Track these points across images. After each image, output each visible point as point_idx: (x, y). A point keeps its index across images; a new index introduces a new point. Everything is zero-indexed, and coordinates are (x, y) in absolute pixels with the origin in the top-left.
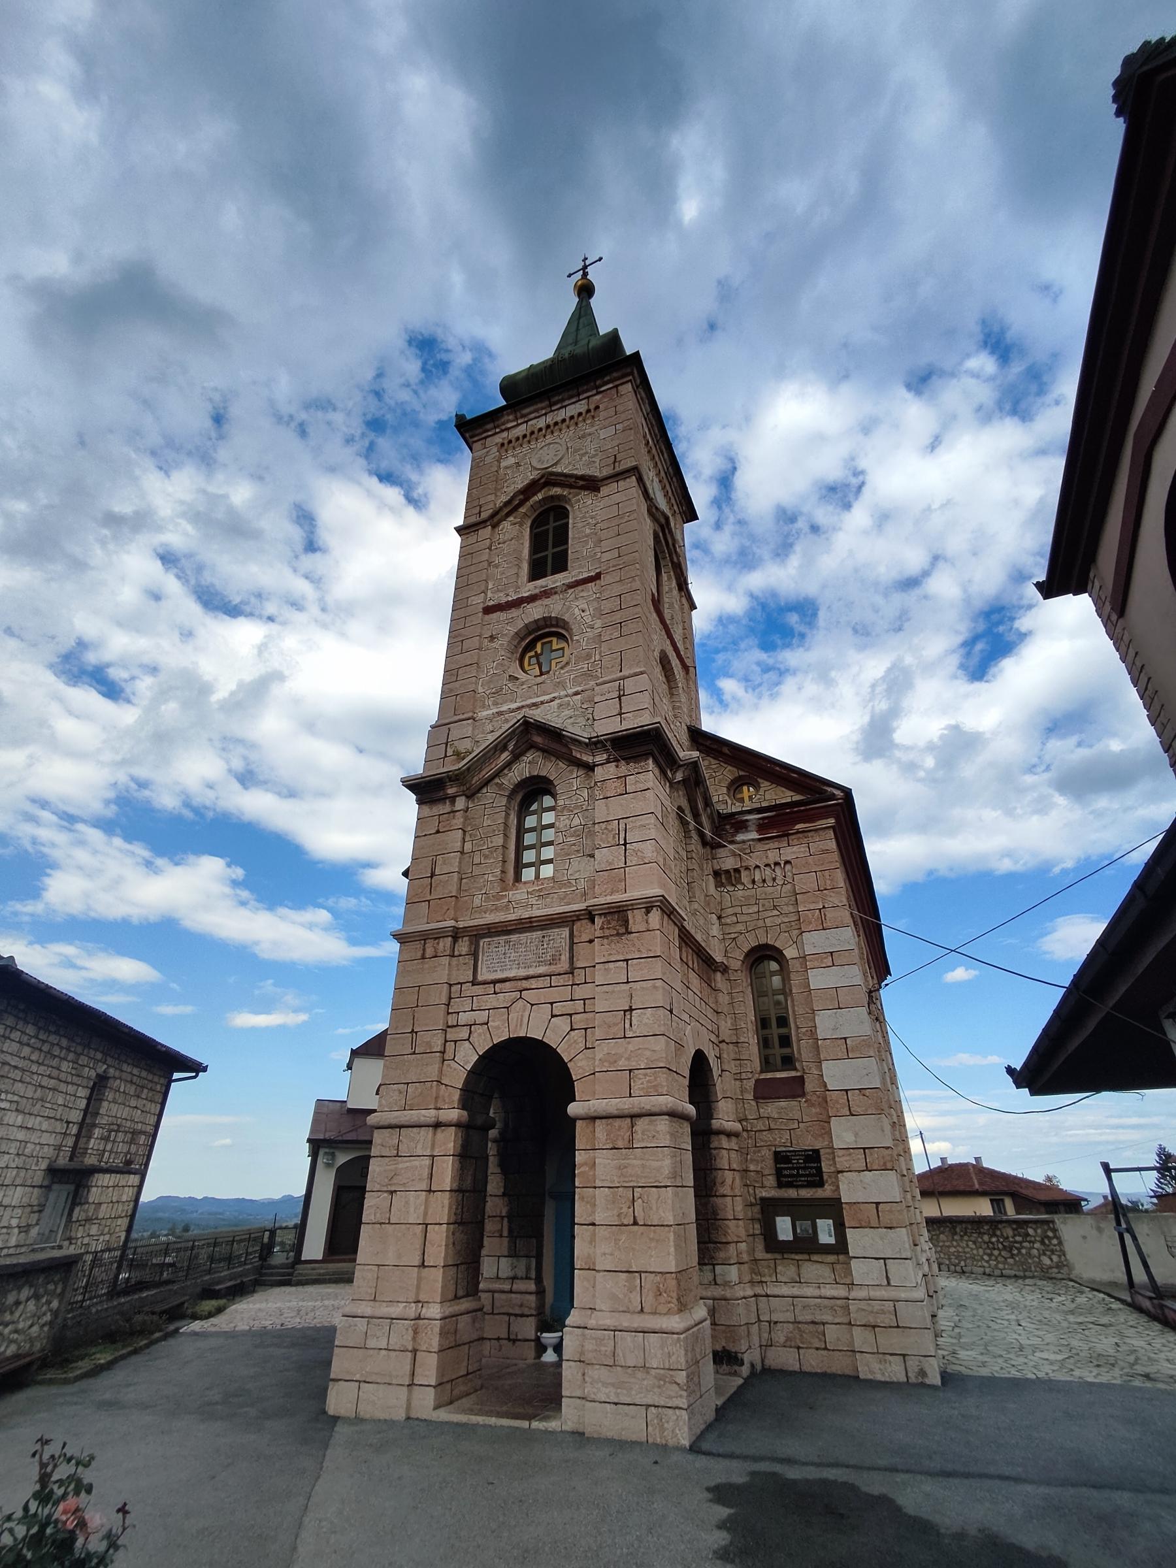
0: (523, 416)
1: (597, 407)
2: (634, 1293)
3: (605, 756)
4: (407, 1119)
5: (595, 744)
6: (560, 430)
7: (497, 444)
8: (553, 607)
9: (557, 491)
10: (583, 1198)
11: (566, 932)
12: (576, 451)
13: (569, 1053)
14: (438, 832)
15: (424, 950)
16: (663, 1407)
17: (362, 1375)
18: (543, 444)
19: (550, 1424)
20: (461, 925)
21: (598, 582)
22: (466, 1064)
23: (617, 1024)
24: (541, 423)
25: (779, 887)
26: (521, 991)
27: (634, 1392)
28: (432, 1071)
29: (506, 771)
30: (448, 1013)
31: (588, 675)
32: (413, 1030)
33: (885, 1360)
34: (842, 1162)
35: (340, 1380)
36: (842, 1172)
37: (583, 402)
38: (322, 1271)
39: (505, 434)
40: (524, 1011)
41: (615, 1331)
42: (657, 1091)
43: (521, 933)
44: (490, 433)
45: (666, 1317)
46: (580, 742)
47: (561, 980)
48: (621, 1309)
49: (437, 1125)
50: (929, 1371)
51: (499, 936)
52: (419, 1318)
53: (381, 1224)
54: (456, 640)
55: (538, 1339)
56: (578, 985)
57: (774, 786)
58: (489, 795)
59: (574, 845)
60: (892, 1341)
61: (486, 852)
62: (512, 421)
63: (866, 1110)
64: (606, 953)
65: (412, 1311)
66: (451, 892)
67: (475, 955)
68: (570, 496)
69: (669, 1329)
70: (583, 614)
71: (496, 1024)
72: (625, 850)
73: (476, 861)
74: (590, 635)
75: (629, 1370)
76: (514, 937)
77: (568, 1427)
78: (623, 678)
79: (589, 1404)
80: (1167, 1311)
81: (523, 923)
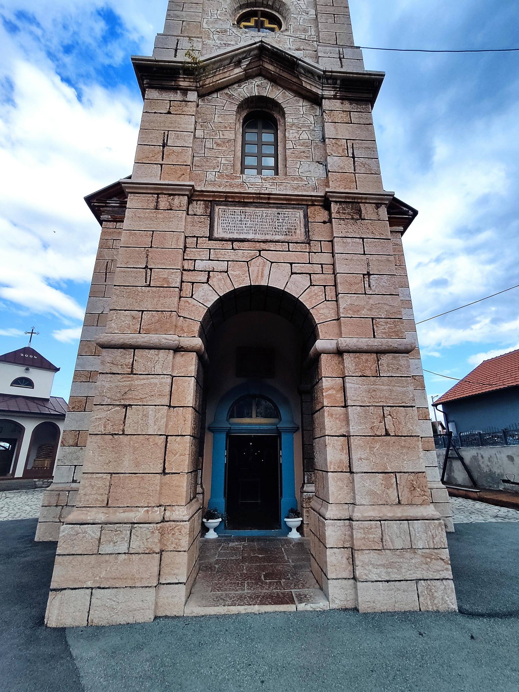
2: (391, 490)
3: (332, 93)
11: (300, 214)
13: (311, 302)
14: (169, 113)
15: (157, 202)
17: (95, 581)
19: (318, 605)
22: (206, 302)
26: (260, 251)
27: (404, 570)
28: (172, 302)
29: (235, 86)
30: (184, 259)
32: (146, 267)
35: (65, 589)
40: (264, 266)
41: (380, 521)
43: (257, 207)
47: (299, 247)
48: (380, 503)
49: (178, 349)
52: (163, 521)
55: (203, 523)
56: (315, 253)
59: (304, 152)
61: (219, 141)
64: (343, 231)
65: (157, 514)
66: (185, 162)
69: (430, 516)
71: (237, 273)
72: (354, 161)
73: (208, 145)
74: (306, 17)
76: (249, 210)
77: (336, 604)
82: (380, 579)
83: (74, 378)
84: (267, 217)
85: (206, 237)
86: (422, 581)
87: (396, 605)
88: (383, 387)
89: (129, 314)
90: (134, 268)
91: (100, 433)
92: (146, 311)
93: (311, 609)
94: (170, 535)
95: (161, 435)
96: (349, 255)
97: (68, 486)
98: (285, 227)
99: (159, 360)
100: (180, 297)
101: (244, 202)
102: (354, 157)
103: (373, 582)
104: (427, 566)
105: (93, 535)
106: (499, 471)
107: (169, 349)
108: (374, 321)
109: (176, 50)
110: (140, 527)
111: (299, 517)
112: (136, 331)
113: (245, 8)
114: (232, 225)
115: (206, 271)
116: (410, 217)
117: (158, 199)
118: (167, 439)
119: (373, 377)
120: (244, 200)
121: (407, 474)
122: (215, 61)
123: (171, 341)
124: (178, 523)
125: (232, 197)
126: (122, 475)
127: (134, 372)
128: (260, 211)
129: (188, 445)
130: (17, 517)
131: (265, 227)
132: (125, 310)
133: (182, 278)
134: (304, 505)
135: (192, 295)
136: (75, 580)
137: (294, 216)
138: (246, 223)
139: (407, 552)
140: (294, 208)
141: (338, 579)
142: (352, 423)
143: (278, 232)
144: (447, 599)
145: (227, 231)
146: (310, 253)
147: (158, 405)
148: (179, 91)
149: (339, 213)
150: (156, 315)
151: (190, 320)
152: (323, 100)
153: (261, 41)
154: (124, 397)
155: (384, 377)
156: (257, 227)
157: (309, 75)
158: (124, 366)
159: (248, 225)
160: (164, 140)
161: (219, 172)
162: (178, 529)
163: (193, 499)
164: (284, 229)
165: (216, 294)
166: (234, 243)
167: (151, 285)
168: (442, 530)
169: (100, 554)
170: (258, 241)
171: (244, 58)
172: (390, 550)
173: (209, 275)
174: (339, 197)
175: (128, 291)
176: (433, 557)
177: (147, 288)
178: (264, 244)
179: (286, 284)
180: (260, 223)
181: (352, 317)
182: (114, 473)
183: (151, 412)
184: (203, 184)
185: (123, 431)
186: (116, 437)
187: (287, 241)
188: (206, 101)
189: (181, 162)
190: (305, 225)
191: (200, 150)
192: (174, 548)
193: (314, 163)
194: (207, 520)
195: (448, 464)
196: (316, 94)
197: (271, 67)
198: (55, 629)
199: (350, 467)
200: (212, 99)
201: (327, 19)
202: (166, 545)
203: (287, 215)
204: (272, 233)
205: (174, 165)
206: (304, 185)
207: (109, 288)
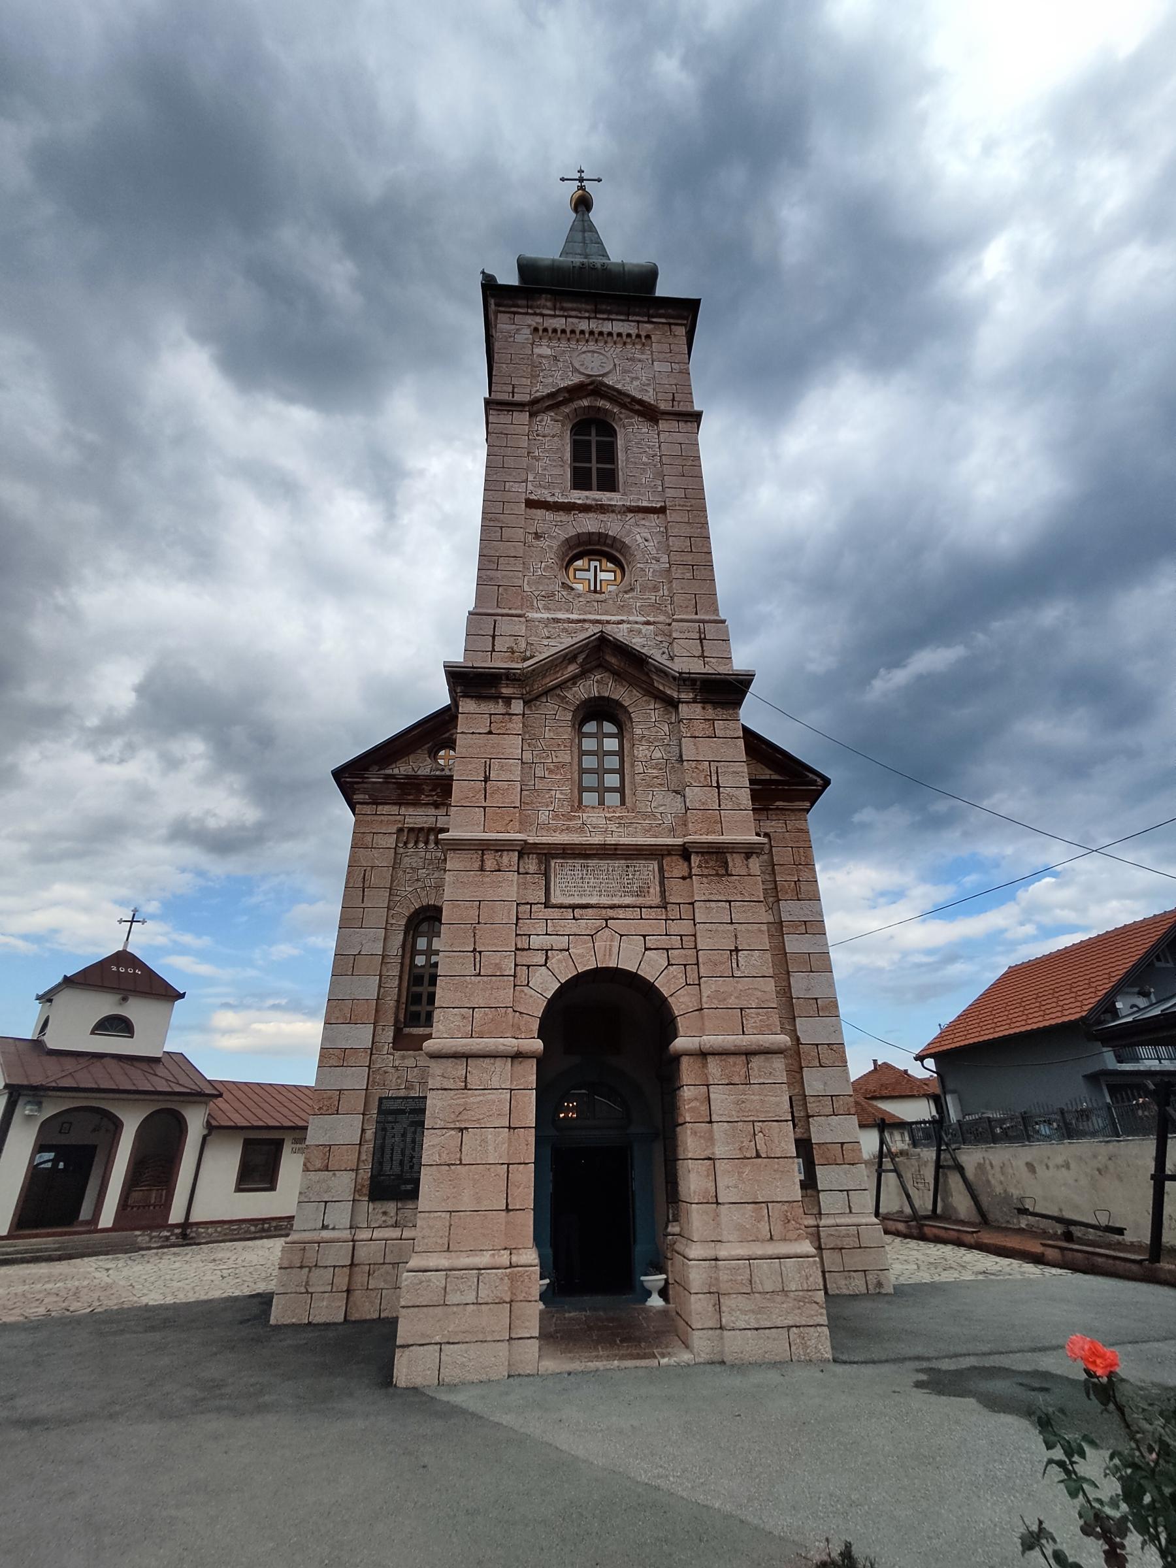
0: (562, 309)
1: (648, 337)
3: (691, 695)
5: (686, 680)
6: (606, 342)
7: (529, 326)
8: (612, 526)
9: (601, 403)
10: (696, 1133)
11: (654, 865)
12: (625, 371)
14: (490, 733)
15: (482, 861)
16: (804, 1326)
18: (585, 349)
20: (531, 840)
21: (660, 515)
22: (545, 992)
24: (584, 325)
26: (606, 920)
28: (505, 995)
29: (569, 684)
31: (657, 607)
32: (475, 950)
33: (850, 1277)
34: (812, 1107)
35: (412, 1345)
36: (813, 1116)
37: (633, 324)
39: (539, 319)
40: (612, 940)
42: (771, 1030)
44: (520, 310)
46: (666, 674)
47: (653, 913)
48: (751, 1239)
49: (518, 1056)
50: (884, 1282)
51: (575, 858)
53: (448, 1165)
54: (492, 524)
56: (673, 920)
57: (754, 762)
58: (549, 707)
59: (656, 777)
60: (856, 1260)
62: (548, 309)
63: (834, 1062)
64: (706, 892)
65: (504, 1258)
66: (513, 802)
67: (546, 875)
68: (622, 416)
70: (646, 544)
73: (539, 773)
75: (768, 1296)
76: (592, 863)
78: (704, 622)
79: (725, 1332)
80: (926, 1230)
81: (607, 849)
82: (748, 1327)
83: (320, 1060)
86: (794, 1328)
87: (766, 1356)
88: (752, 1096)
91: (435, 1163)
93: (675, 1364)
94: (519, 1283)
95: (502, 1164)
97: (315, 1236)
100: (515, 986)
102: (718, 787)
103: (740, 1330)
104: (800, 1311)
105: (438, 1283)
106: (1018, 1192)
107: (506, 1057)
109: (494, 637)
110: (488, 1274)
111: (661, 1274)
112: (468, 1034)
113: (575, 549)
115: (543, 950)
116: (819, 788)
117: (482, 857)
122: (545, 663)
124: (527, 1269)
126: (462, 1213)
127: (469, 1087)
128: (604, 864)
130: (182, 1298)
132: (454, 1008)
134: (669, 1254)
135: (528, 982)
136: (423, 1335)
139: (778, 1295)
144: (821, 1347)
148: (500, 701)
149: (702, 867)
152: (680, 705)
153: (602, 631)
154: (459, 1119)
157: (662, 674)
158: (457, 1080)
159: (591, 884)
160: (485, 772)
168: (817, 1270)
171: (581, 652)
172: (760, 1293)
173: (547, 955)
174: (700, 848)
176: (807, 1300)
182: (454, 1212)
183: (490, 1136)
184: (535, 829)
185: (461, 1160)
186: (453, 1167)
188: (533, 708)
189: (508, 803)
190: (660, 883)
191: (529, 781)
193: (668, 792)
195: (941, 1180)
196: (672, 698)
197: (613, 660)
198: (407, 1388)
199: (716, 1196)
200: (540, 705)
201: (682, 573)
202: (515, 1294)
205: (499, 807)
207: (368, 912)
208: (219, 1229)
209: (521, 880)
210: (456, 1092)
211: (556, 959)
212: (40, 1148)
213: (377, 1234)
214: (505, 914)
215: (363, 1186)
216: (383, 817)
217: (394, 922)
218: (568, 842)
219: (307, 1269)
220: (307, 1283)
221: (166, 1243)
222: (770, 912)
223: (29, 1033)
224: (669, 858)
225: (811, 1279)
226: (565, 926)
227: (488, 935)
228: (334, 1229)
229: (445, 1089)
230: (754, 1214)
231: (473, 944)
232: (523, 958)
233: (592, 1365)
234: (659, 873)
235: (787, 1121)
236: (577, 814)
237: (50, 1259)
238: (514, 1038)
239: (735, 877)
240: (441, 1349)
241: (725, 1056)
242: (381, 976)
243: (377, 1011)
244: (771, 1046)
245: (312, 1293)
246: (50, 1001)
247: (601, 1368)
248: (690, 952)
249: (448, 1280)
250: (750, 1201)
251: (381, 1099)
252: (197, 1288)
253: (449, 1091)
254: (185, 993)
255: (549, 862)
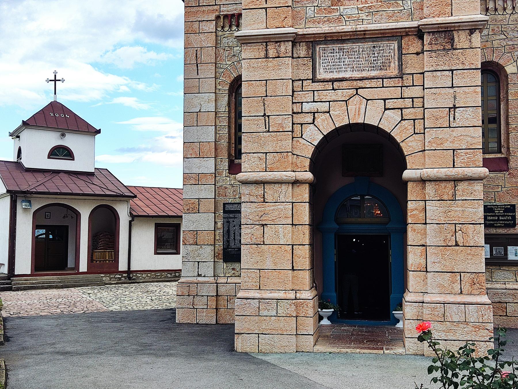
2: (456, 284)
4: (271, 177)
11: (395, 45)
13: (401, 137)
15: (267, 50)
20: (300, 32)
23: (444, 117)
25: (508, 16)
26: (357, 89)
28: (287, 144)
32: (265, 114)
35: (243, 333)
38: (34, 282)
40: (360, 104)
41: (444, 304)
45: (478, 296)
47: (392, 82)
49: (296, 183)
53: (257, 244)
56: (407, 87)
65: (292, 295)
75: (455, 324)
76: (347, 46)
77: (411, 351)
82: (440, 339)
84: (363, 53)
85: (310, 79)
88: (457, 208)
89: (257, 156)
90: (255, 116)
91: (249, 243)
92: (268, 153)
94: (301, 308)
95: (289, 245)
96: (437, 89)
97: (194, 279)
98: (380, 61)
99: (282, 191)
100: (293, 138)
101: (341, 40)
107: (289, 183)
108: (455, 152)
114: (332, 64)
118: (293, 247)
119: (450, 200)
120: (341, 37)
121: (470, 274)
123: (290, 178)
125: (331, 37)
127: (266, 201)
128: (356, 46)
129: (308, 251)
131: (361, 63)
132: (254, 153)
133: (293, 120)
135: (302, 135)
137: (389, 48)
138: (344, 60)
139: (462, 324)
140: (388, 40)
141: (413, 338)
142: (428, 237)
143: (373, 67)
145: (328, 70)
146: (403, 88)
147: (285, 224)
150: (276, 156)
151: (302, 157)
154: (261, 219)
155: (459, 200)
156: (354, 64)
159: (346, 63)
161: (317, 6)
162: (306, 304)
163: (312, 288)
164: (379, 63)
165: (321, 133)
166: (334, 83)
167: (270, 131)
169: (260, 316)
170: (355, 80)
173: (314, 116)
175: (253, 136)
176: (481, 328)
177: (268, 133)
178: (361, 82)
179: (380, 121)
180: (357, 59)
181: (436, 150)
182: (261, 269)
183: (280, 229)
184: (304, 22)
185: (264, 242)
186: (259, 246)
187: (381, 76)
190: (398, 59)
192: (304, 315)
194: (322, 310)
199: (426, 268)
203: (382, 48)
204: (368, 69)
205: (276, 7)
206: (399, 11)
208: (149, 275)
209: (295, 63)
210: (259, 204)
211: (320, 119)
212: (36, 226)
213: (229, 280)
214: (284, 89)
215: (219, 254)
216: (204, 8)
217: (220, 87)
218: (328, 31)
219: (192, 296)
220: (193, 304)
221: (119, 281)
222: (515, 64)
223: (12, 158)
224: (407, 39)
225: (486, 317)
226: (327, 95)
227: (273, 104)
228: (204, 276)
229: (252, 202)
230: (450, 279)
231: (263, 111)
232: (298, 119)
233: (344, 350)
234: (399, 51)
235: (480, 224)
236: (335, 8)
237: (57, 287)
238: (294, 171)
239: (459, 51)
240: (258, 336)
241: (438, 182)
242: (216, 126)
243: (216, 149)
244: (474, 176)
245: (196, 309)
246: (18, 137)
247: (350, 352)
248: (419, 110)
249: (260, 304)
250: (449, 271)
251: (224, 204)
252: (138, 305)
253: (254, 203)
254: (100, 130)
255: (315, 48)
